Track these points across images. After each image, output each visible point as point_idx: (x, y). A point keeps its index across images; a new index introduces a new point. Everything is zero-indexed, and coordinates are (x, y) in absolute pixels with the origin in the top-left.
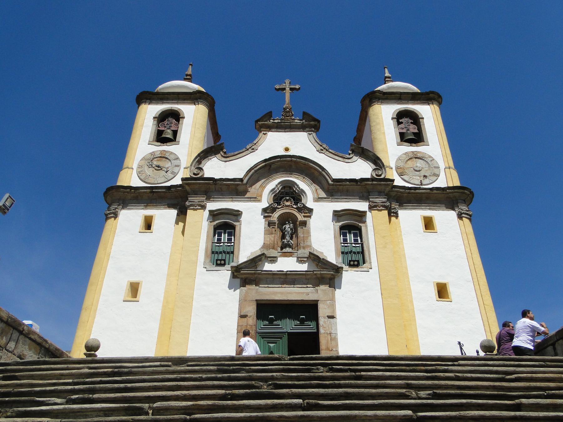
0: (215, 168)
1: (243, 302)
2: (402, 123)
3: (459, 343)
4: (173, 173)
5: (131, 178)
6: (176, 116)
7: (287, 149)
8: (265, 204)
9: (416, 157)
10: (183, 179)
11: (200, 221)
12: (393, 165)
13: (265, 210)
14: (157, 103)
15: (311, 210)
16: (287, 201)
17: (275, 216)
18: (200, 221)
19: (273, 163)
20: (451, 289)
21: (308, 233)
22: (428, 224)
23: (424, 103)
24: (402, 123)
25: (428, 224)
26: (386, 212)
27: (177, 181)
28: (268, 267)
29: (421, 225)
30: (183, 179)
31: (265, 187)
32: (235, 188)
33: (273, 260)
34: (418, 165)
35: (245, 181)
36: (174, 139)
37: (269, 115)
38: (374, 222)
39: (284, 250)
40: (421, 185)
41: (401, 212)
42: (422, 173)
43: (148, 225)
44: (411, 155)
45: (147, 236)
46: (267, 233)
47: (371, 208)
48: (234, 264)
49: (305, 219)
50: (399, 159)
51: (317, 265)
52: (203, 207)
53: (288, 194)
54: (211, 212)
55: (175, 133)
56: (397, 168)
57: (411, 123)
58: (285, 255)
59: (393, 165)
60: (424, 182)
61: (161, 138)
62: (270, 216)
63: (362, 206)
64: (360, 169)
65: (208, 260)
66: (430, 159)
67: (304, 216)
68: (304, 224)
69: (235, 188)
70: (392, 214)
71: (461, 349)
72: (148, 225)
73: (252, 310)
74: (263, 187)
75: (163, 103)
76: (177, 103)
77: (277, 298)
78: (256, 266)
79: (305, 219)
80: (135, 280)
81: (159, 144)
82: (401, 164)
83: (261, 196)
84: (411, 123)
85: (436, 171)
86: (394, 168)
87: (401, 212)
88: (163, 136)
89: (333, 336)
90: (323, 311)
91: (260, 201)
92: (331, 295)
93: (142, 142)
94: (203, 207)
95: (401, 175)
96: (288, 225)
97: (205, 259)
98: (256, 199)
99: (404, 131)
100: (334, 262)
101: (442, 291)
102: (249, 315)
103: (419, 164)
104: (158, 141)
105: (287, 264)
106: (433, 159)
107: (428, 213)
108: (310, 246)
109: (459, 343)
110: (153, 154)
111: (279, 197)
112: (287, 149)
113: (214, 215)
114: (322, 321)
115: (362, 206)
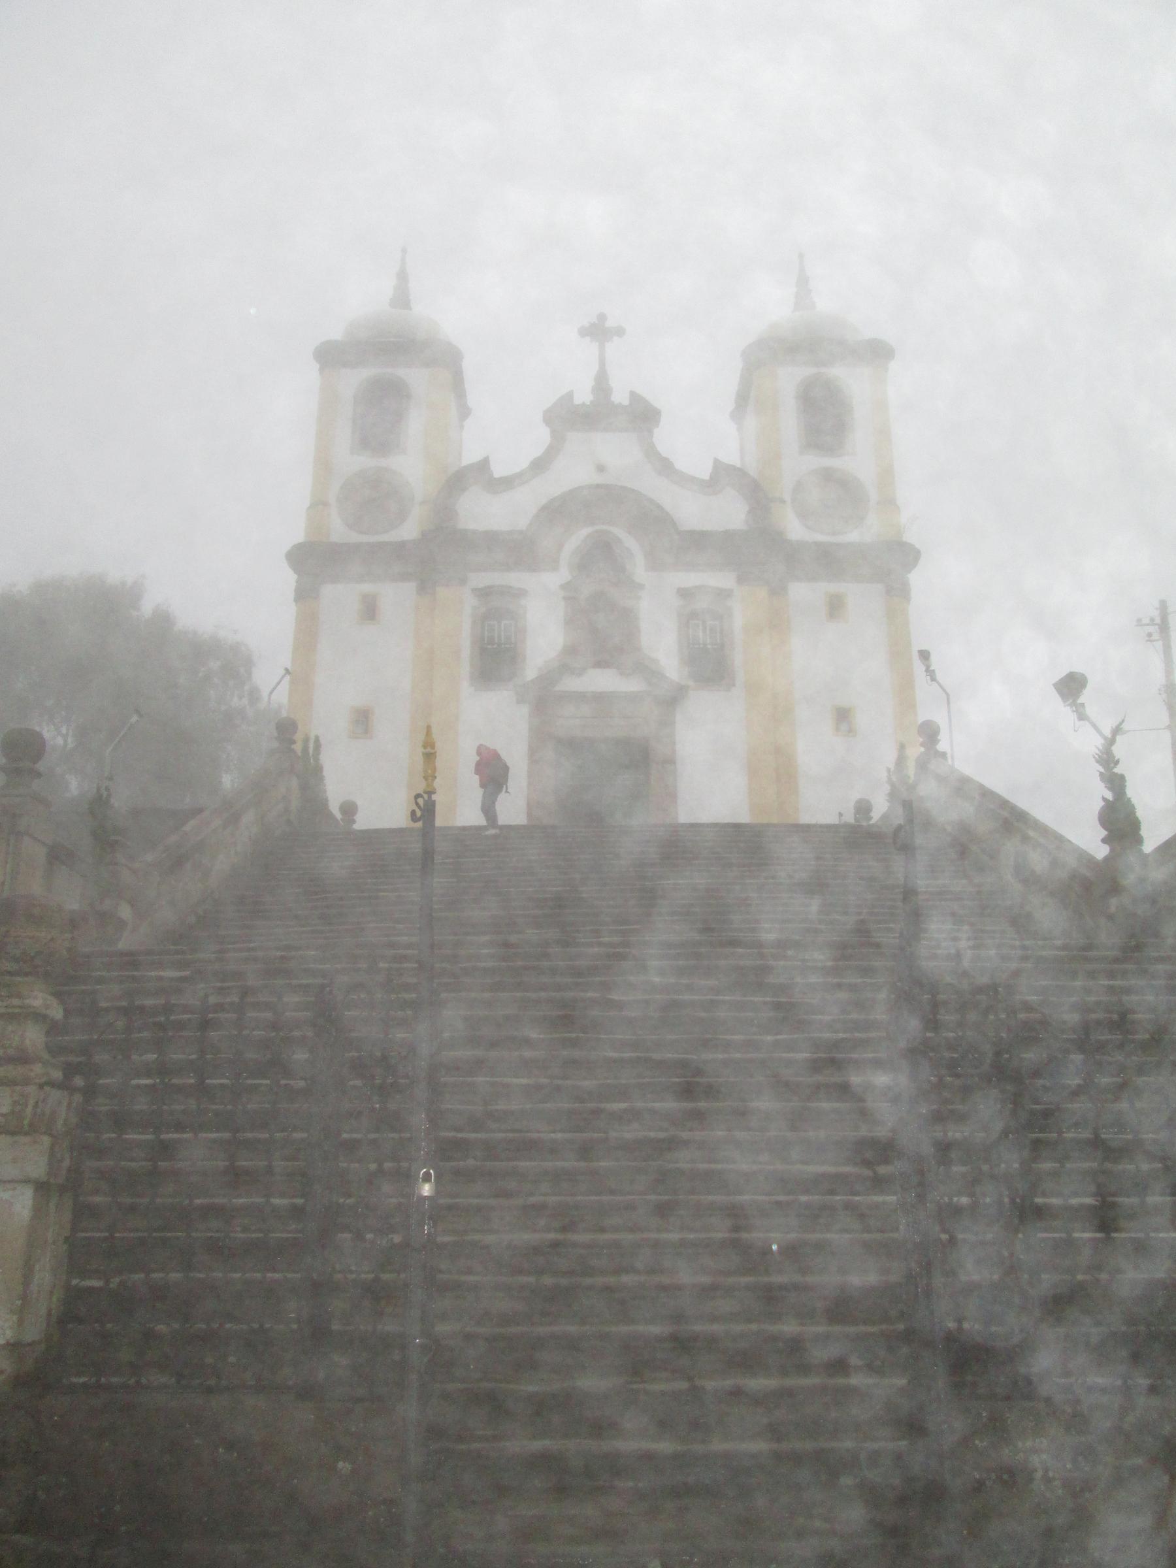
8: (565, 574)
37: (570, 396)
47: (740, 580)
54: (474, 590)
72: (370, 611)
94: (463, 581)
96: (603, 633)
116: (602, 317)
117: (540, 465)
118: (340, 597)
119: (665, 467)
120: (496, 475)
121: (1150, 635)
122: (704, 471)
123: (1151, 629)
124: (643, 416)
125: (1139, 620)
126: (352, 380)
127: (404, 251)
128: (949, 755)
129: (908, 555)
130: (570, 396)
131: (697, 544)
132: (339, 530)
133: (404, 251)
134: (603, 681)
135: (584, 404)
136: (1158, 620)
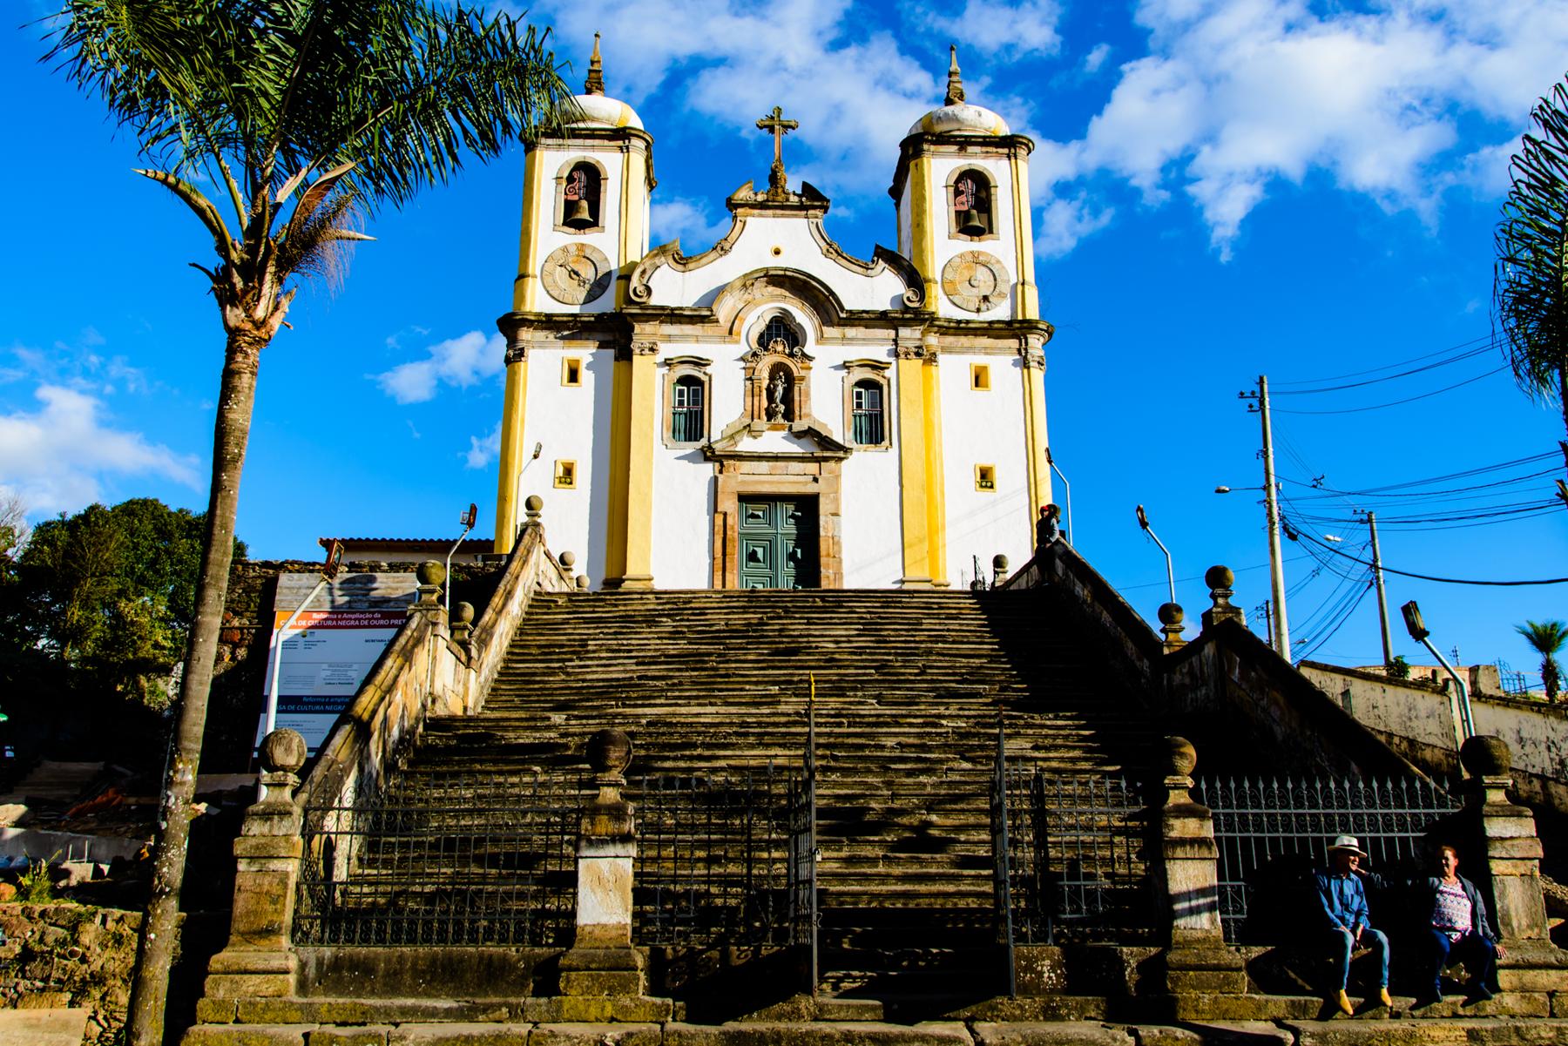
5: (537, 301)
8: (742, 349)
9: (976, 260)
15: (810, 359)
20: (998, 477)
21: (808, 395)
22: (979, 380)
36: (594, 222)
38: (904, 377)
40: (978, 310)
51: (819, 444)
53: (782, 330)
61: (572, 220)
79: (803, 373)
82: (949, 276)
91: (737, 342)
93: (547, 236)
101: (985, 478)
107: (980, 360)
108: (809, 415)
113: (668, 363)
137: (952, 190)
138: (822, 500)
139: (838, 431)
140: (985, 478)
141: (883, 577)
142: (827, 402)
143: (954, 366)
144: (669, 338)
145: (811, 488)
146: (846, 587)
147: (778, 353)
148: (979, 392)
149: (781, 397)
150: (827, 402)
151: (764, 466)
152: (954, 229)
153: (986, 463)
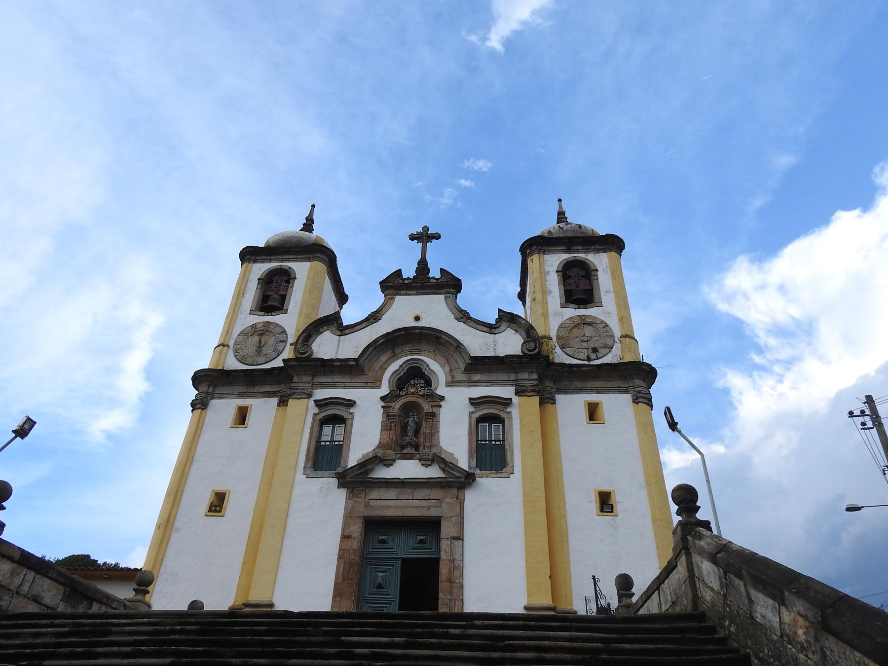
0: (326, 346)
1: (348, 517)
2: (570, 277)
3: (594, 578)
4: (275, 350)
6: (287, 277)
7: (417, 318)
8: (385, 390)
9: (584, 322)
10: (284, 360)
11: (302, 412)
12: (553, 334)
13: (383, 399)
14: (263, 261)
15: (442, 398)
16: (414, 385)
17: (397, 405)
18: (302, 412)
19: (398, 337)
20: (617, 499)
22: (593, 412)
23: (598, 251)
24: (570, 277)
25: (593, 412)
26: (536, 399)
27: (278, 363)
28: (383, 473)
29: (584, 413)
30: (284, 360)
31: (386, 369)
32: (350, 370)
33: (388, 463)
34: (587, 333)
35: (361, 362)
37: (398, 273)
38: (522, 413)
39: (405, 451)
40: (589, 359)
41: (560, 398)
42: (592, 345)
43: (242, 417)
44: (578, 321)
45: (240, 432)
46: (385, 427)
47: (517, 393)
48: (339, 470)
49: (434, 410)
50: (561, 326)
52: (309, 396)
55: (283, 299)
56: (558, 338)
57: (582, 276)
58: (406, 457)
59: (553, 334)
60: (593, 356)
62: (390, 407)
63: (506, 392)
64: (510, 343)
65: (310, 464)
66: (603, 325)
67: (432, 407)
68: (433, 416)
69: (350, 370)
70: (547, 400)
71: (595, 584)
72: (242, 417)
73: (357, 529)
74: (383, 369)
75: (270, 261)
76: (288, 260)
77: (390, 514)
78: (367, 472)
79: (434, 410)
80: (220, 488)
81: (263, 313)
82: (564, 333)
83: (381, 380)
84: (582, 276)
85: (609, 341)
86: (554, 339)
87: (560, 398)
88: (269, 303)
89: (457, 563)
90: (447, 530)
91: (379, 386)
92: (458, 510)
94: (309, 396)
95: (562, 347)
97: (306, 463)
98: (375, 383)
99: (573, 287)
100: (466, 468)
101: (605, 502)
102: (354, 535)
103: (588, 331)
104: (261, 310)
105: (407, 469)
106: (607, 326)
107: (594, 398)
108: (437, 445)
109: (594, 578)
110: (254, 326)
111: (401, 382)
112: (417, 318)
113: (319, 404)
114: (444, 544)
115: (506, 392)
116: (426, 229)
117: (374, 318)
118: (224, 408)
119: (464, 317)
120: (345, 323)
121: (863, 424)
122: (491, 318)
123: (861, 419)
124: (450, 285)
125: (851, 414)
126: (261, 269)
127: (313, 206)
128: (713, 525)
129: (648, 374)
130: (398, 273)
131: (483, 367)
132: (232, 363)
133: (313, 206)
134: (407, 469)
135: (409, 278)
136: (868, 412)
137: (561, 274)
138: (444, 525)
139: (464, 461)
140: (605, 502)
141: (513, 602)
142: (454, 435)
143: (570, 406)
144: (322, 386)
145: (433, 513)
146: (281, 605)
147: (413, 391)
148: (595, 427)
149: (410, 425)
150: (454, 435)
151: (392, 493)
152: (564, 301)
153: (605, 488)
